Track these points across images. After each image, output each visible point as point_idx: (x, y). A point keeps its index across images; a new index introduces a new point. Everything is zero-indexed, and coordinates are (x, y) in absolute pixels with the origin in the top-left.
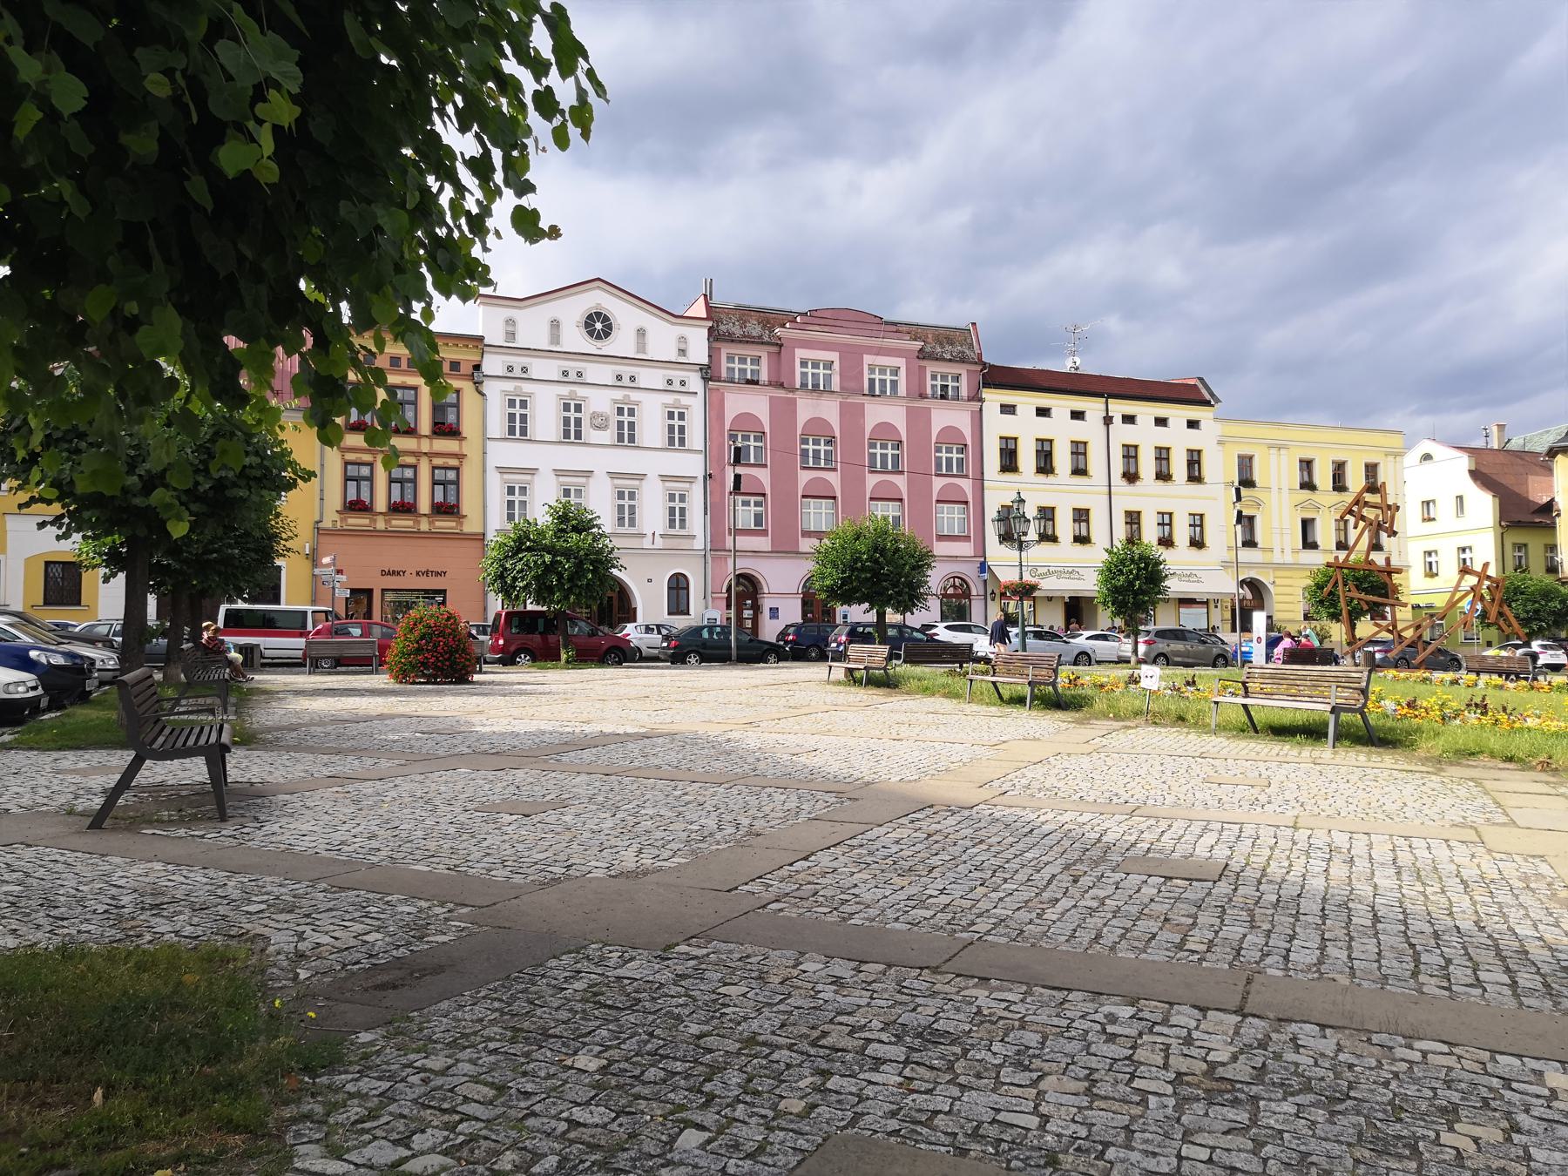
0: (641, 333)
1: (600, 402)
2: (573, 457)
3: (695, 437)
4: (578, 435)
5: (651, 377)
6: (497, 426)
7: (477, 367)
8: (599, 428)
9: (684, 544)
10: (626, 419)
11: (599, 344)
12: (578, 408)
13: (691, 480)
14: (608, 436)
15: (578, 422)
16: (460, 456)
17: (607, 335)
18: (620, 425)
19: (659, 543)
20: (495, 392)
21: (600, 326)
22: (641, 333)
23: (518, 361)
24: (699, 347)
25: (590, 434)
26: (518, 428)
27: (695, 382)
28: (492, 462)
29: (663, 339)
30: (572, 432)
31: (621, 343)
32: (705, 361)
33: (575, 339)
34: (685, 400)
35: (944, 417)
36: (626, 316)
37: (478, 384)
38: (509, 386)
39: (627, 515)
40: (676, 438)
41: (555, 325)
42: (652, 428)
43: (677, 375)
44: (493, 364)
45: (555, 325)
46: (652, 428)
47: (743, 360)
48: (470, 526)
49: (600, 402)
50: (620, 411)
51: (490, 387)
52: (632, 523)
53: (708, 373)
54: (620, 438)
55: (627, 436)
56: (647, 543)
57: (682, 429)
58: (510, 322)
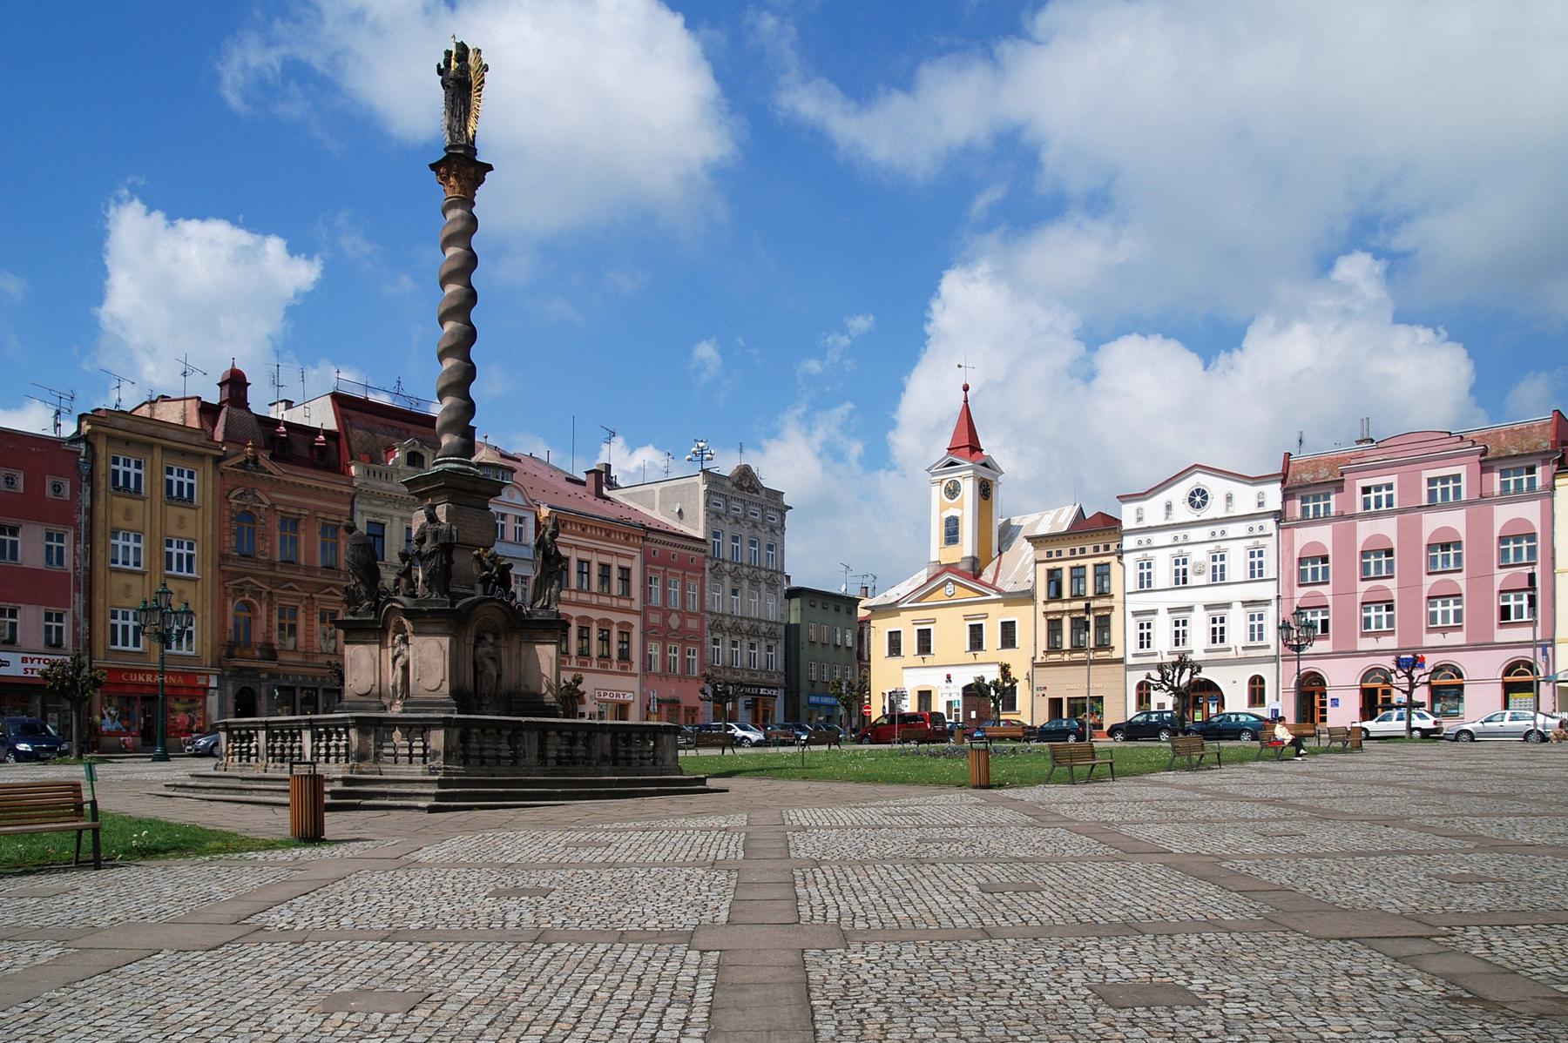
0: (1229, 498)
1: (1199, 555)
2: (1182, 598)
3: (1270, 570)
4: (1185, 581)
5: (1235, 529)
6: (1132, 583)
8: (1199, 573)
9: (1262, 653)
10: (1218, 563)
11: (1198, 512)
12: (1185, 562)
13: (1266, 602)
14: (1206, 578)
15: (1185, 572)
16: (1112, 608)
17: (1204, 504)
18: (1214, 568)
19: (1241, 653)
21: (1198, 498)
22: (1229, 498)
23: (1143, 537)
24: (1273, 496)
25: (1193, 580)
26: (1145, 583)
27: (1270, 524)
28: (1130, 608)
29: (1246, 498)
30: (1181, 580)
31: (1215, 509)
32: (1279, 507)
33: (1183, 513)
34: (1262, 541)
35: (1503, 515)
36: (1217, 487)
37: (1120, 558)
38: (1139, 555)
39: (1218, 635)
40: (1256, 573)
41: (1169, 507)
42: (1237, 566)
43: (1255, 524)
44: (1129, 542)
45: (1169, 507)
46: (1237, 566)
47: (1316, 498)
48: (1116, 654)
49: (1199, 555)
50: (1214, 559)
52: (1222, 640)
53: (1279, 516)
54: (1214, 578)
55: (1218, 577)
56: (1231, 655)
57: (1261, 565)
58: (1139, 511)
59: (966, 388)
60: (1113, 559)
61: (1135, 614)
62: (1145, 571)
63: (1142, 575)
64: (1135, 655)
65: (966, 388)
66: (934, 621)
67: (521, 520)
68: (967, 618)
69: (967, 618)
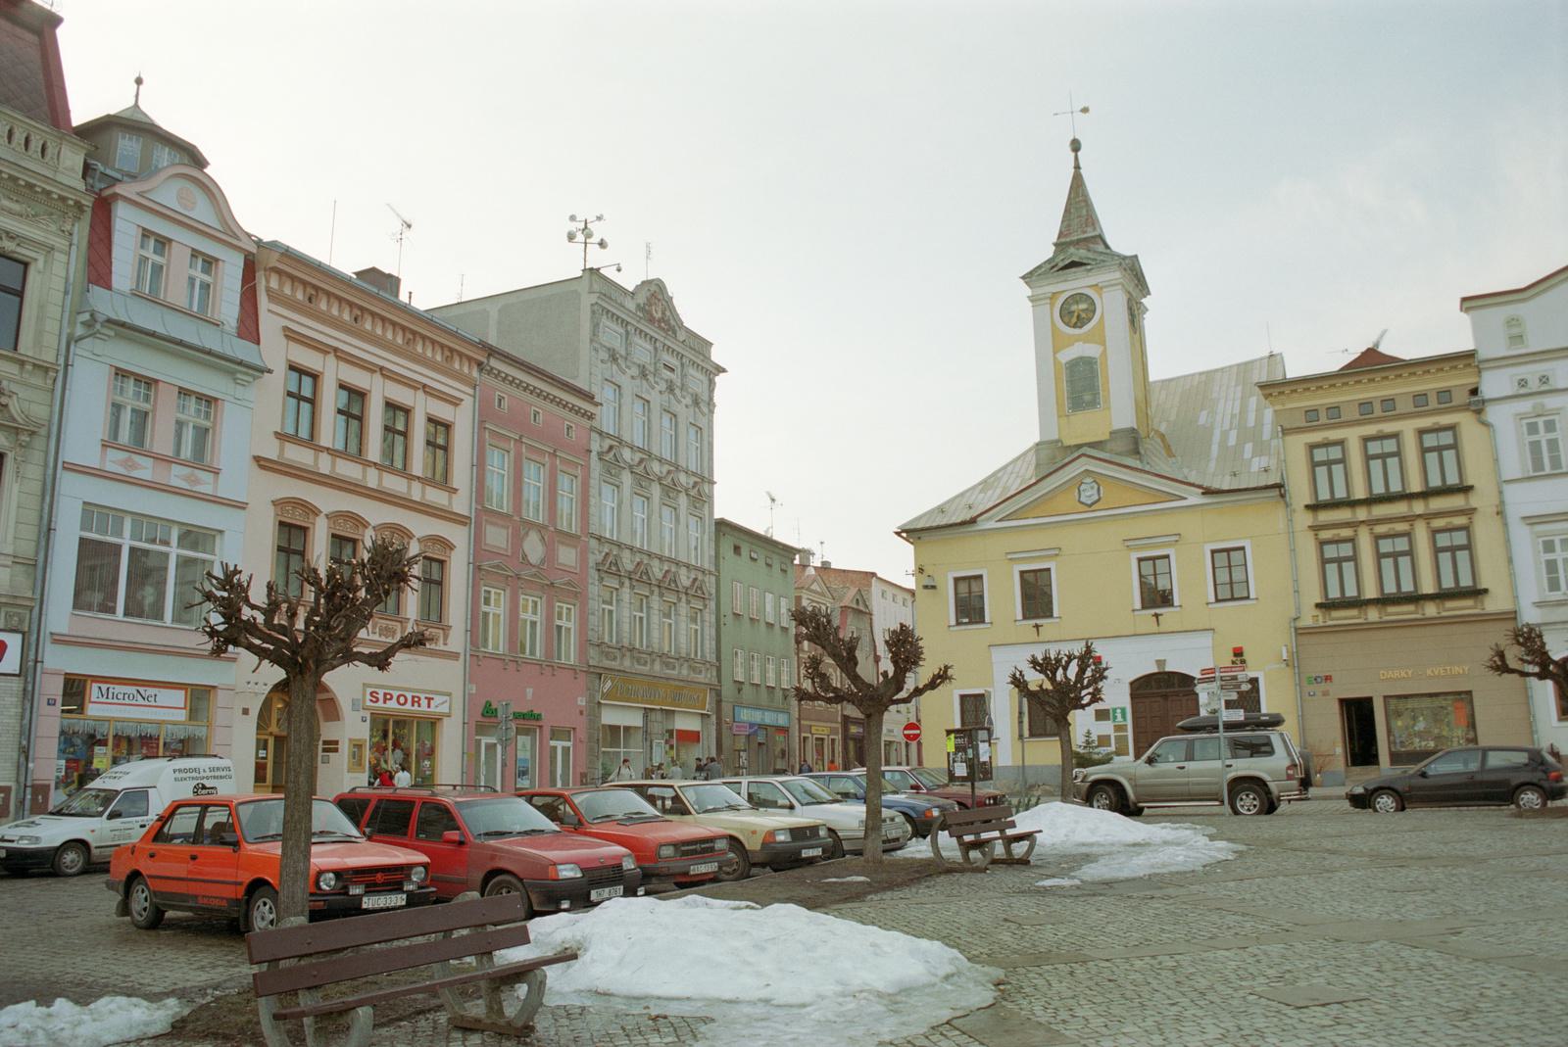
6: (1514, 462)
7: (1474, 392)
20: (1500, 416)
23: (1531, 372)
28: (1514, 513)
44: (1493, 384)
48: (1493, 604)
51: (1492, 413)
59: (1076, 146)
60: (1465, 420)
61: (1531, 520)
62: (1543, 437)
63: (1535, 447)
64: (1539, 605)
65: (1076, 146)
66: (1056, 553)
67: (210, 263)
68: (1129, 543)
69: (1129, 543)
